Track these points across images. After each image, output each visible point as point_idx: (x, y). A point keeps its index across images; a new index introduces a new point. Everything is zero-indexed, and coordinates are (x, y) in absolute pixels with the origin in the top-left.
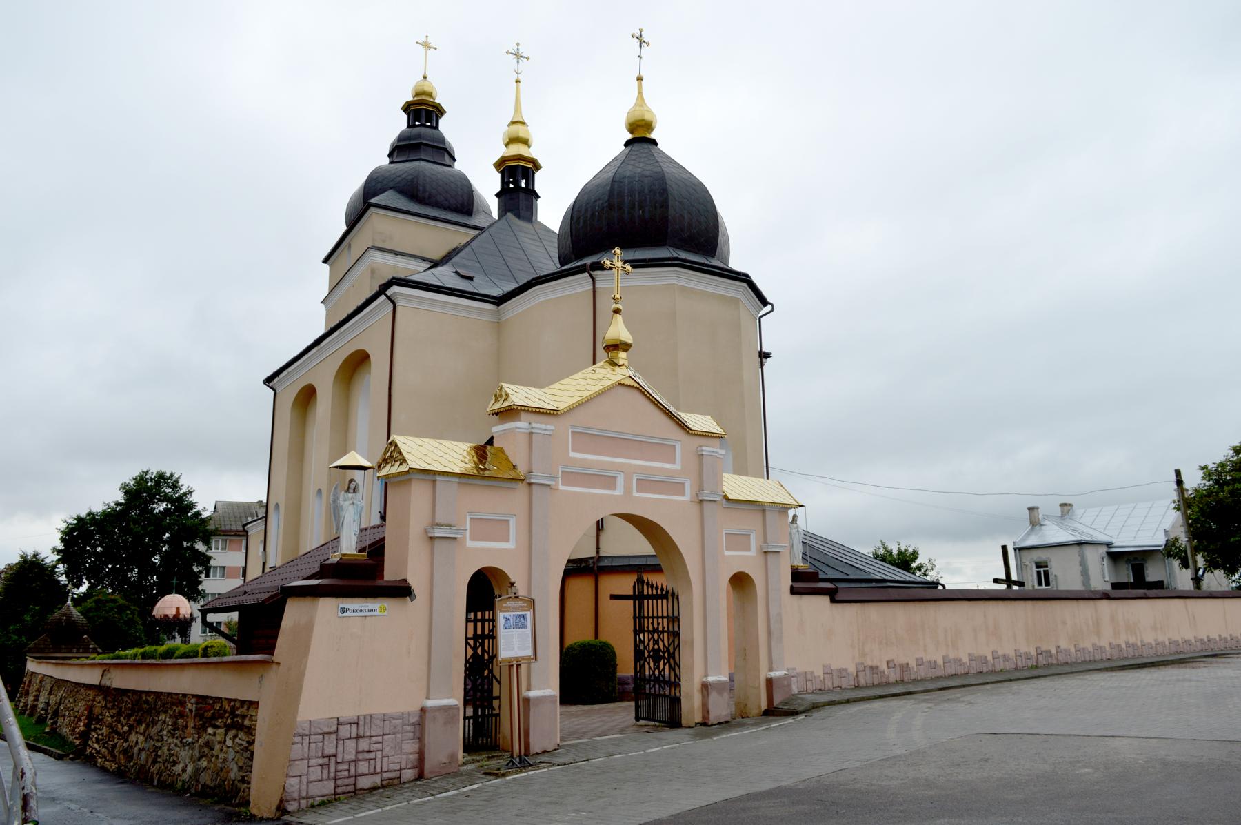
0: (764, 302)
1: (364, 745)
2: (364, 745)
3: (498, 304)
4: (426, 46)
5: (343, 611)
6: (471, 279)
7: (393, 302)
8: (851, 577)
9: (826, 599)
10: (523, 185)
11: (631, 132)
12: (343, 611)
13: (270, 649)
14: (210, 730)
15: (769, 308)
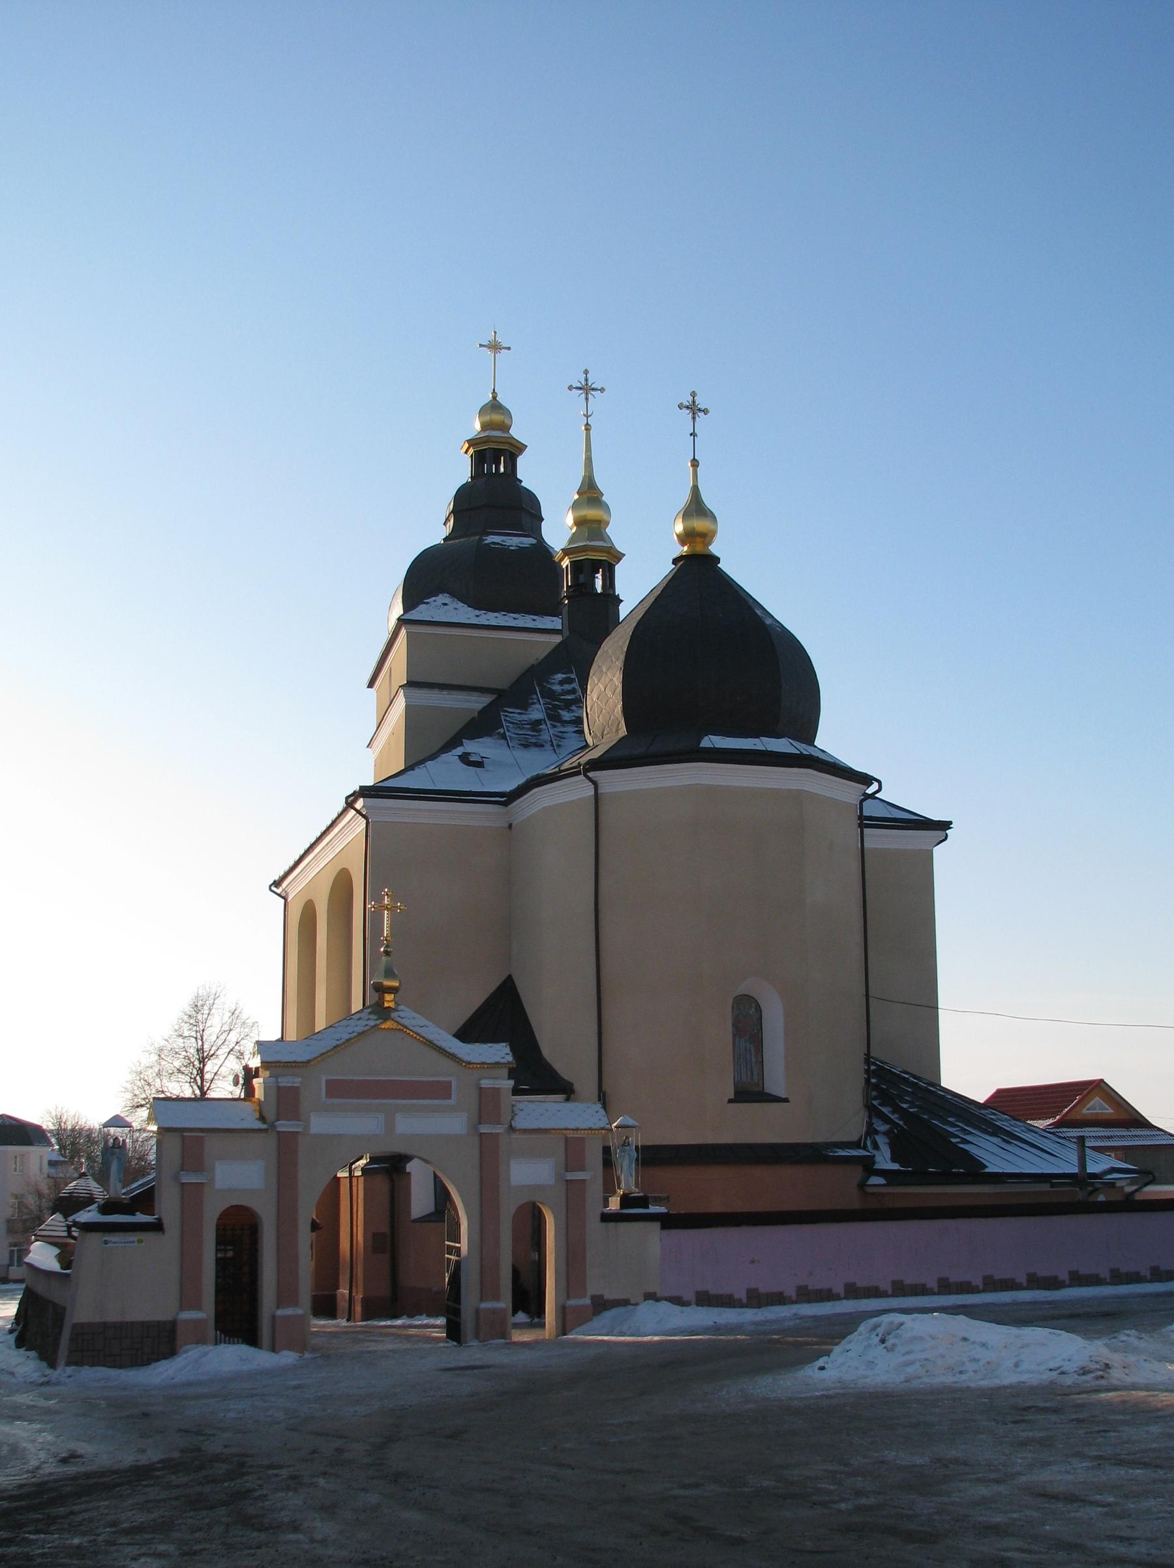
0: (867, 780)
4: (495, 347)
5: (106, 1242)
9: (656, 1226)
11: (683, 544)
12: (106, 1242)
15: (874, 787)
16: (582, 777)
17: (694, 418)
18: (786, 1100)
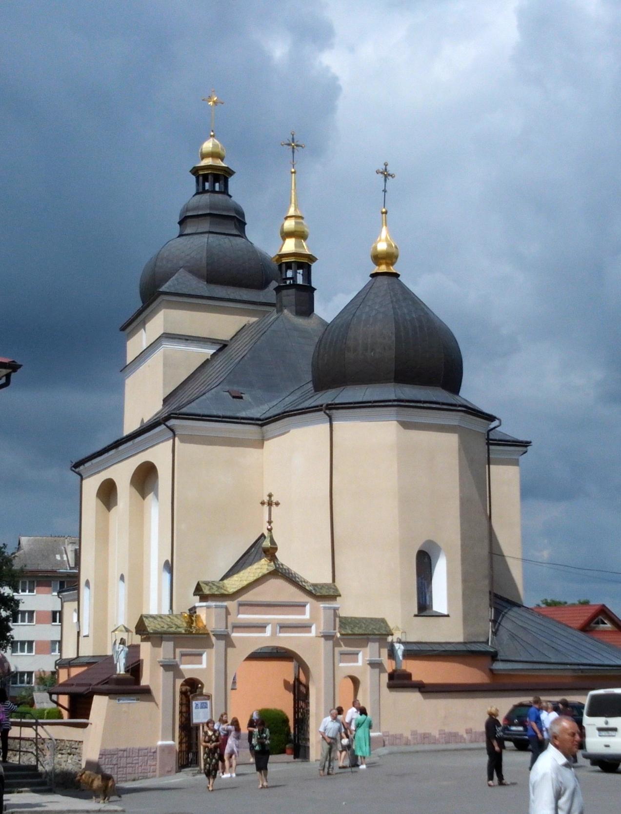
0: (491, 418)
1: (129, 760)
2: (129, 760)
3: (262, 425)
6: (241, 398)
7: (172, 430)
8: (553, 661)
10: (300, 280)
13: (87, 716)
14: (60, 756)
16: (322, 413)
17: (385, 181)
18: (448, 616)
